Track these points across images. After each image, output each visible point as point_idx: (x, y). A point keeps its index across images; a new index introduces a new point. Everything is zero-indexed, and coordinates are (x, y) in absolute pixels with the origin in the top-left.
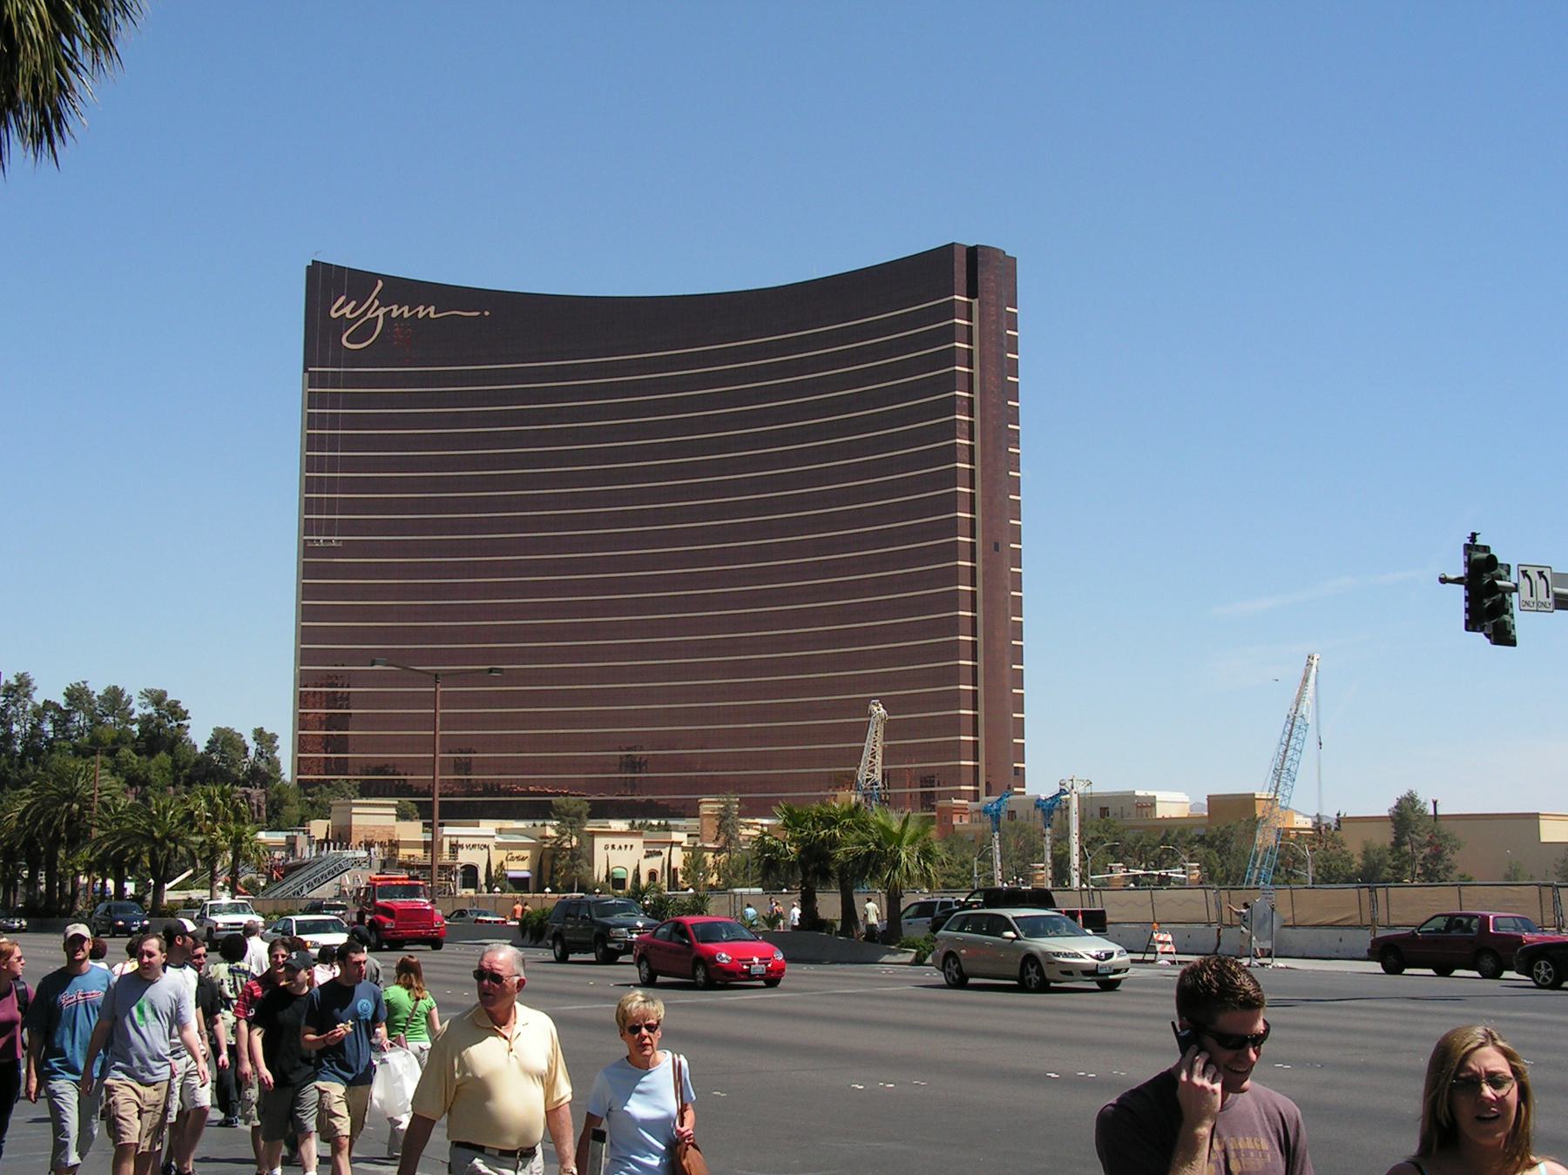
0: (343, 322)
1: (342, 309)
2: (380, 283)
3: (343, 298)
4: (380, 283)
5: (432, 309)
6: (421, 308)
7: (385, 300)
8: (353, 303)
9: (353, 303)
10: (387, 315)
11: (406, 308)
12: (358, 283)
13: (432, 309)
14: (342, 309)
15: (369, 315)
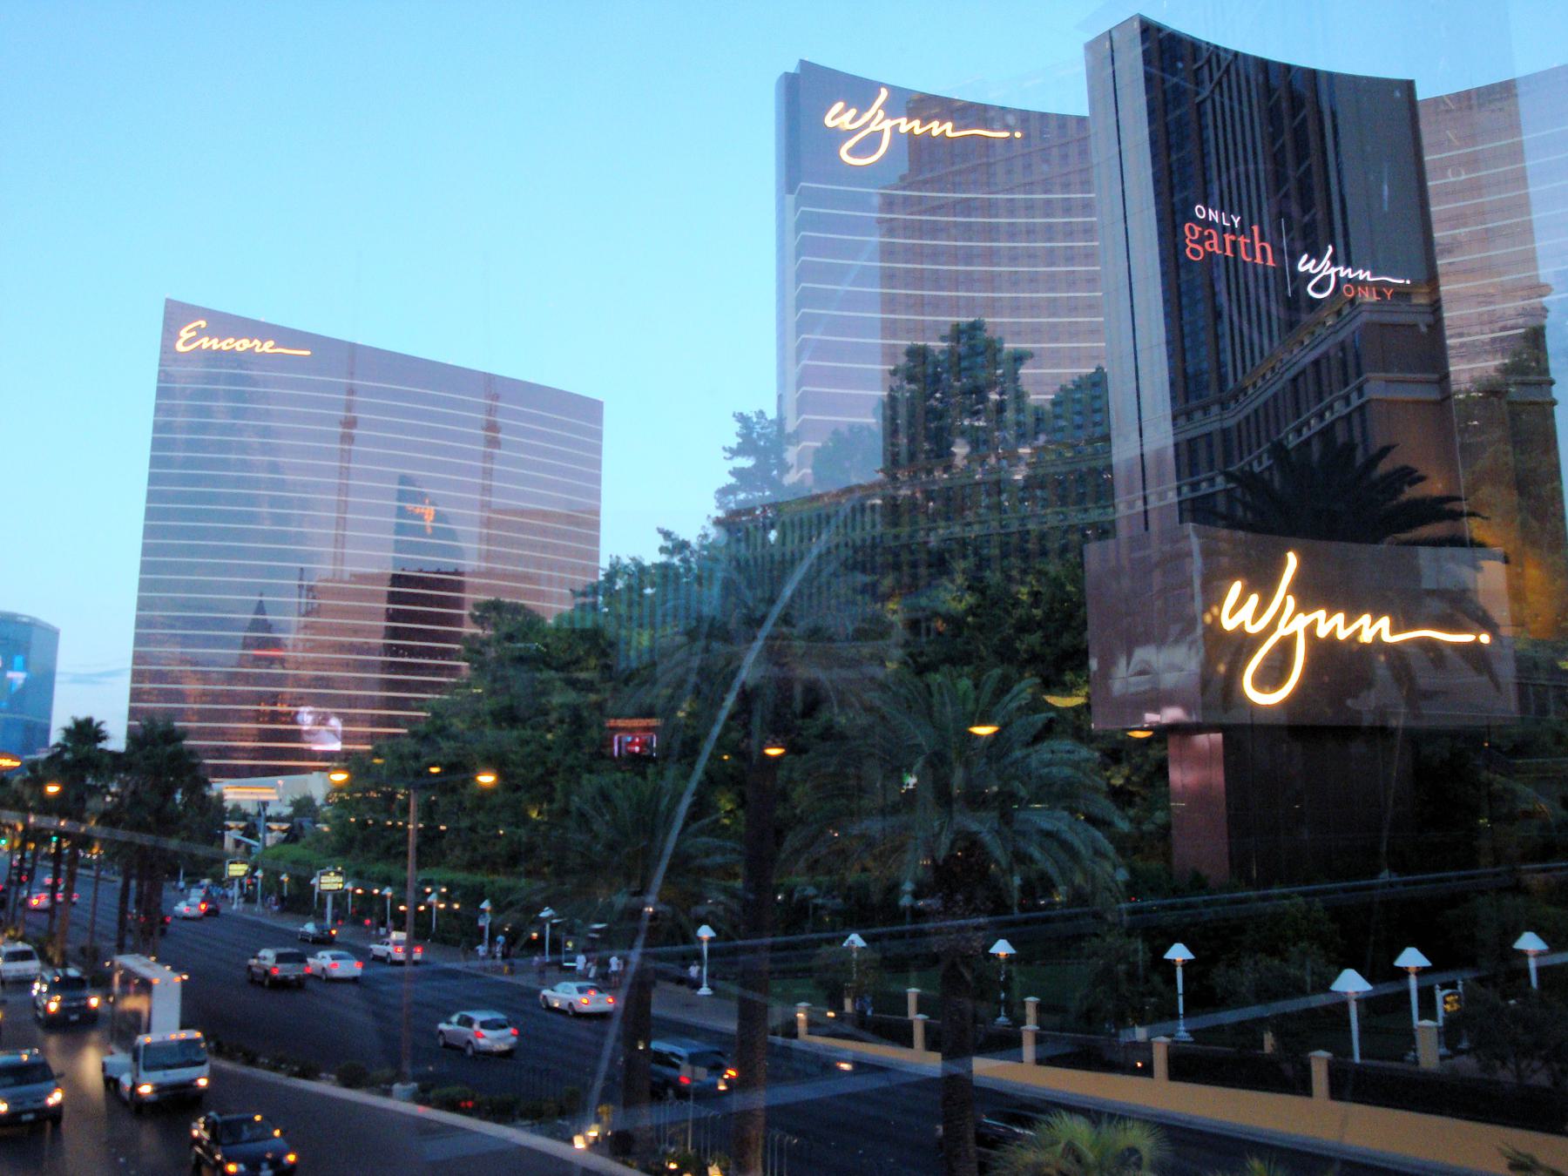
0: (840, 136)
1: (838, 117)
2: (884, 93)
3: (839, 106)
4: (884, 93)
5: (948, 126)
6: (935, 124)
7: (890, 110)
8: (853, 112)
9: (853, 112)
10: (895, 129)
11: (916, 123)
12: (859, 92)
13: (948, 126)
14: (838, 117)
15: (873, 128)
